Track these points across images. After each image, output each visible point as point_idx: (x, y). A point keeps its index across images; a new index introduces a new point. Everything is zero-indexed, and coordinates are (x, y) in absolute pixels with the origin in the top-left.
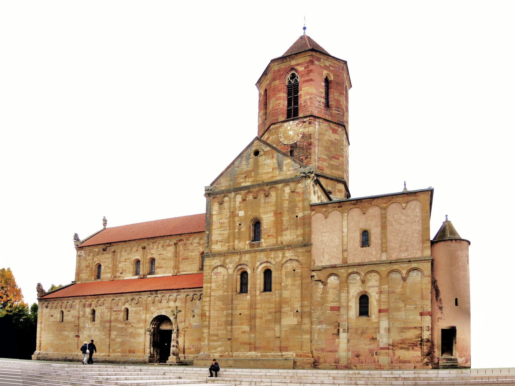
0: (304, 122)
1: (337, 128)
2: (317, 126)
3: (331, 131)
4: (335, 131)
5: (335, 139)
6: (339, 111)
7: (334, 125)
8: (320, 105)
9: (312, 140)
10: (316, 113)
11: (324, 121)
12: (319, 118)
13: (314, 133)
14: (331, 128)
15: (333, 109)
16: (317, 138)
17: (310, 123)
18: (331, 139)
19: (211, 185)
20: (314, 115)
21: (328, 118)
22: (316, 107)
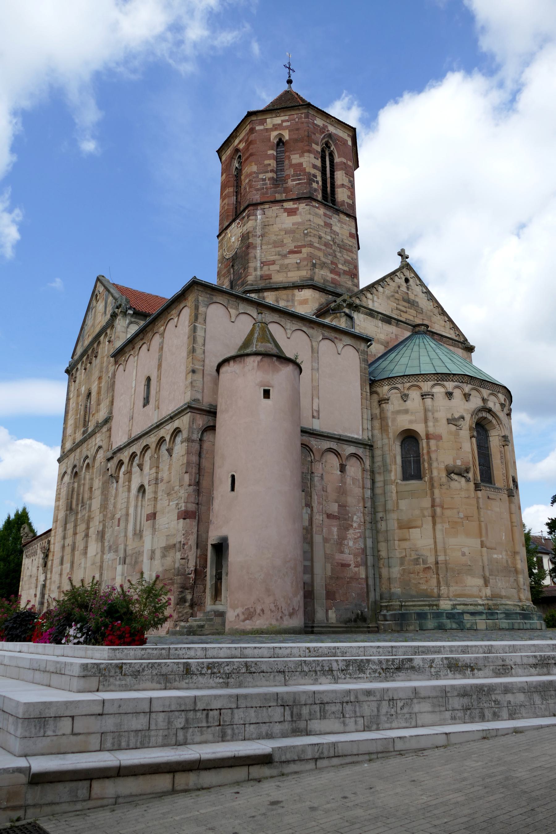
0: (244, 218)
1: (296, 206)
2: (259, 217)
3: (286, 214)
4: (292, 212)
5: (293, 224)
6: (299, 179)
7: (291, 203)
8: (266, 184)
9: (250, 240)
10: (257, 198)
11: (271, 205)
12: (262, 203)
13: (255, 228)
14: (286, 210)
15: (289, 180)
16: (259, 233)
17: (248, 216)
18: (284, 226)
19: (72, 358)
20: (254, 202)
21: (278, 197)
22: (257, 190)
